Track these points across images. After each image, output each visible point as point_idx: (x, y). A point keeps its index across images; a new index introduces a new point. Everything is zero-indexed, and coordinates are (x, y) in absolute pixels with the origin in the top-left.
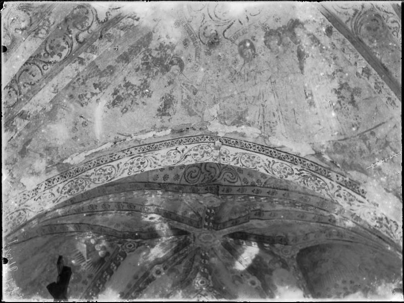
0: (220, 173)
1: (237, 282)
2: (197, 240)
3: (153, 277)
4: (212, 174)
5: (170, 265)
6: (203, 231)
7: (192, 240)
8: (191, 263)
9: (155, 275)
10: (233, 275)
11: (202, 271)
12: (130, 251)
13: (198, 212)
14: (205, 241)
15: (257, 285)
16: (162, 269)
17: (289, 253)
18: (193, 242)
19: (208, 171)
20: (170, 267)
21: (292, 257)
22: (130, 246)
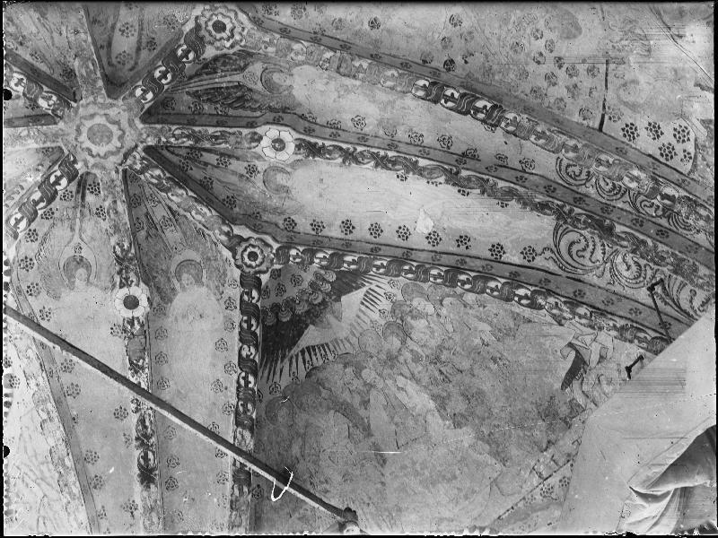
2: (129, 143)
3: (298, 147)
5: (241, 133)
6: (91, 161)
8: (219, 64)
9: (291, 147)
11: (191, 56)
13: (78, 192)
14: (114, 128)
16: (265, 142)
20: (245, 131)
22: (253, 256)
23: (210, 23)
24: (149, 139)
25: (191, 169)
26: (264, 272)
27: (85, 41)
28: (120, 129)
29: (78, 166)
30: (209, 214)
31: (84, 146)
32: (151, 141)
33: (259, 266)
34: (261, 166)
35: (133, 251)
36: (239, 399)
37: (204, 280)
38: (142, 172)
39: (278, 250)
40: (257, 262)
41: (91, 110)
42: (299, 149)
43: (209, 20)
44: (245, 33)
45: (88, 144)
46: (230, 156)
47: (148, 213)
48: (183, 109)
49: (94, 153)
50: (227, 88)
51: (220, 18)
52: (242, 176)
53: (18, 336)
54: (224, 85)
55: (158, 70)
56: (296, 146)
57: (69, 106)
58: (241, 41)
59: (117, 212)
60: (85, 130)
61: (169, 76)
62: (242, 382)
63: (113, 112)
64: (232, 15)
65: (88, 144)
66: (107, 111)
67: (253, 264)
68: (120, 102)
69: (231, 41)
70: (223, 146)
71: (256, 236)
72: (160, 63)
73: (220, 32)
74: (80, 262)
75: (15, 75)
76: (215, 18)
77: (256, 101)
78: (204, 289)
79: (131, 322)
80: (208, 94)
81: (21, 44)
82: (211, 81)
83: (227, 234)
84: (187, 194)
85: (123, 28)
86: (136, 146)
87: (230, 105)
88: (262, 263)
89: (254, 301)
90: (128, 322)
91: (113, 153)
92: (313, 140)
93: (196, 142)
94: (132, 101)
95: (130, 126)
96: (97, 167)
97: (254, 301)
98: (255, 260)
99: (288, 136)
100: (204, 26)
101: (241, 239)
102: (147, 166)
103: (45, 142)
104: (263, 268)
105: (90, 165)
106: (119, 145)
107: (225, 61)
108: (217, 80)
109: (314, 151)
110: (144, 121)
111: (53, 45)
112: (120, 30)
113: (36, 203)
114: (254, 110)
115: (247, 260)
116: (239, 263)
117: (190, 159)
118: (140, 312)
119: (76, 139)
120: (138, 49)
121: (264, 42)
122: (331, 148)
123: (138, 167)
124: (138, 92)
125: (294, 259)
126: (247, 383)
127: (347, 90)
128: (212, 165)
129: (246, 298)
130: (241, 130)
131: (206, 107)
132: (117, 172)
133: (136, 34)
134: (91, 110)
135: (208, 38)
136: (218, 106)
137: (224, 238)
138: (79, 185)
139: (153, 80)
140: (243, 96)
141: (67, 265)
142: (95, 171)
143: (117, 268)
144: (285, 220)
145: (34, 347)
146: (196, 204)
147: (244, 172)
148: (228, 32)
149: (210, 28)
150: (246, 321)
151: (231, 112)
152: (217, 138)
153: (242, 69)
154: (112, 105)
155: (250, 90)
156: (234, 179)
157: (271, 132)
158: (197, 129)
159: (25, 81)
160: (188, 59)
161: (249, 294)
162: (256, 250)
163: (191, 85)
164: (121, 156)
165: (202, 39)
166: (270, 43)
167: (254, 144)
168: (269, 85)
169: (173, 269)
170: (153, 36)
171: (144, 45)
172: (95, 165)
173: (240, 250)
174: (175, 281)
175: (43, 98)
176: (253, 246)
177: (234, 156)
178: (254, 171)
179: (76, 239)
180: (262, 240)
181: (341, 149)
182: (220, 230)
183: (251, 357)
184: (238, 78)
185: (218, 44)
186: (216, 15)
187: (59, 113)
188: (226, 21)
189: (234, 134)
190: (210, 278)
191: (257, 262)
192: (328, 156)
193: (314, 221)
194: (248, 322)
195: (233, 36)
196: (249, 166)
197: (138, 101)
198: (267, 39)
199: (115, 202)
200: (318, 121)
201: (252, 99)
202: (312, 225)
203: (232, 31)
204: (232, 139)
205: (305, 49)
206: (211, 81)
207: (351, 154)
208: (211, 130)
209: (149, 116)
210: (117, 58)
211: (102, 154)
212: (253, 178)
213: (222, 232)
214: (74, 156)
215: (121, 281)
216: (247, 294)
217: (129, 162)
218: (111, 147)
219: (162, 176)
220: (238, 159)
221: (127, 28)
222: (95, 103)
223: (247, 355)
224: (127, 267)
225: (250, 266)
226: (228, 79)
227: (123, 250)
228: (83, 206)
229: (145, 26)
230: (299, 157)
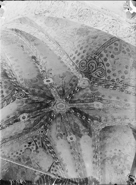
0: (95, 70)
1: (59, 137)
3: (20, 120)
4: (90, 70)
6: (62, 102)
9: (21, 119)
10: (59, 133)
11: (46, 125)
14: (58, 108)
15: (73, 140)
16: (27, 117)
18: (52, 106)
19: (89, 67)
21: (99, 130)
26: (17, 93)
30: (34, 99)
32: (50, 108)
38: (51, 102)
39: (16, 99)
40: (19, 94)
41: (63, 111)
45: (63, 104)
46: (32, 103)
51: (42, 133)
61: (49, 120)
63: (59, 111)
65: (63, 104)
68: (58, 113)
79: (47, 78)
83: (28, 97)
86: (53, 106)
91: (58, 103)
93: (41, 111)
94: (56, 114)
101: (25, 97)
113: (73, 93)
115: (22, 94)
116: (23, 93)
124: (55, 116)
127: (14, 130)
134: (63, 111)
138: (64, 92)
152: (37, 113)
173: (24, 95)
180: (20, 99)
191: (19, 94)
197: (54, 114)
207: (8, 125)
209: (52, 111)
213: (30, 97)
217: (54, 103)
218: (58, 105)
220: (30, 103)
222: (63, 112)
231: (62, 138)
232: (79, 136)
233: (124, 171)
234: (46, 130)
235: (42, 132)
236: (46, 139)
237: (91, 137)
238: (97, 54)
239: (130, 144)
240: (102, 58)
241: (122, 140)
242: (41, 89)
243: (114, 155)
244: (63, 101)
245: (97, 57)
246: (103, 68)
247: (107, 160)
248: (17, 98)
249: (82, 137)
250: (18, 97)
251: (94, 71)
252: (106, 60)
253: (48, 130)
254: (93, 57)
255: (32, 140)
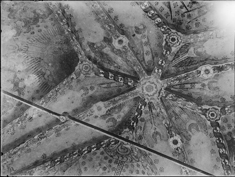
1: (141, 27)
2: (159, 89)
3: (214, 70)
6: (149, 98)
7: (163, 91)
9: (212, 71)
10: (144, 34)
12: (216, 109)
13: (149, 110)
14: (153, 85)
15: (117, 40)
16: (202, 72)
17: (85, 66)
18: (163, 88)
20: (194, 71)
22: (213, 115)
23: (170, 40)
24: (164, 85)
25: (183, 92)
26: (219, 120)
27: (135, 60)
28: (155, 85)
29: (146, 101)
30: (192, 104)
31: (146, 94)
32: (166, 86)
33: (216, 118)
34: (206, 83)
35: (171, 124)
36: (224, 170)
37: (199, 129)
38: (166, 97)
40: (215, 117)
41: (144, 81)
42: (215, 71)
43: (169, 39)
44: (182, 38)
45: (147, 93)
46: (194, 83)
47: (173, 111)
48: (173, 72)
49: (149, 95)
50: (185, 60)
51: (172, 37)
52: (201, 89)
53: (143, 162)
54: (184, 59)
55: (160, 61)
56: (213, 70)
57: (138, 82)
58: (182, 41)
59: (162, 113)
60: (144, 88)
61: (164, 62)
62: (224, 163)
63: (151, 80)
64: (176, 34)
65: (147, 93)
66: (149, 80)
67: (214, 118)
68: (152, 76)
69: (179, 43)
70: (189, 79)
71: (211, 107)
72: (160, 59)
73: (174, 41)
74: (157, 133)
75: (119, 77)
76: (171, 38)
77: (196, 61)
78: (201, 133)
79: (177, 149)
80: (179, 64)
81: (119, 68)
82: (179, 60)
83: (201, 109)
84: (183, 99)
85: (146, 53)
86: (161, 89)
87: (188, 65)
88: (217, 117)
89: (218, 131)
90: (176, 149)
91: (155, 93)
92: (218, 65)
94: (155, 74)
95: (158, 83)
96: (152, 99)
97: (218, 131)
98: (214, 116)
99: (209, 67)
100: (168, 41)
101: (206, 110)
102: (167, 94)
103: (134, 96)
104: (218, 118)
105: (149, 99)
106: (156, 90)
107: (181, 52)
108: (181, 59)
109: (220, 69)
110: (161, 80)
111: (128, 66)
112: (145, 54)
113: (137, 116)
114: (196, 64)
116: (209, 119)
117: (181, 88)
118: (179, 145)
119: (143, 92)
120: (153, 58)
121: (189, 38)
122: (226, 66)
123: (164, 95)
124: (156, 71)
125: (228, 111)
126: (226, 163)
128: (190, 88)
129: (215, 131)
130: (193, 71)
131: (180, 69)
132: (158, 99)
133: (151, 53)
134: (144, 81)
135: (171, 45)
136: (184, 67)
137: (200, 111)
138: (149, 108)
139: (159, 65)
140: (191, 61)
141: (153, 135)
142: (151, 101)
143: (168, 131)
144: (221, 99)
145: (148, 164)
146: (187, 102)
147: (201, 87)
148: (176, 40)
149: (171, 41)
150: (218, 140)
151: (189, 68)
152: (186, 77)
153: (187, 52)
154: (150, 78)
155: (192, 58)
156: (198, 91)
157: (202, 68)
158: (178, 76)
159: (122, 79)
160: (167, 54)
161: (216, 129)
162: (213, 112)
163: (173, 64)
164: (158, 94)
165: (169, 46)
166: (191, 38)
167: (199, 75)
168: (198, 54)
169: (187, 128)
170: (156, 52)
171: (154, 56)
172: (151, 99)
173: (207, 114)
174: (189, 132)
175: (129, 82)
176: (212, 111)
177: (196, 83)
178: (204, 86)
179: (154, 126)
181: (229, 65)
182: (198, 109)
183: (224, 153)
184: (187, 55)
185: (175, 45)
186: (171, 36)
187: (135, 85)
188: (175, 37)
189: (191, 73)
190: (201, 128)
191: (215, 117)
192: (226, 69)
193: (231, 96)
194: (219, 139)
195: (178, 41)
196: (202, 84)
197: (157, 74)
198: (189, 37)
199: (160, 109)
200: (219, 59)
201: (194, 60)
202: (231, 97)
203: (178, 39)
204: (191, 75)
205: (203, 35)
206: (179, 60)
208: (183, 75)
209: (162, 77)
210: (147, 63)
211: (152, 95)
212: (205, 88)
213: (199, 109)
214: (144, 98)
215: (170, 136)
216: (215, 129)
217: (161, 95)
218: (154, 92)
219: (172, 95)
220: (197, 83)
221: (148, 52)
223: (222, 153)
224: (171, 130)
225: (213, 119)
226: (184, 57)
227: (168, 125)
228: (152, 114)
229: (152, 50)
230: (216, 73)
231: (136, 27)
232: (108, 39)
233: (9, 13)
234: (167, 43)
235: (173, 40)
236: (165, 28)
237: (88, 42)
238: (122, 162)
239: (24, 50)
240: (114, 160)
241: (38, 47)
242: (182, 109)
243: (39, 24)
244: (148, 99)
245: (120, 158)
246: (109, 154)
247: (47, 14)
248: (218, 111)
249: (103, 39)
250: (217, 111)
251: (119, 146)
252: (110, 161)
253: (164, 44)
254: (125, 158)
255: (189, 9)
